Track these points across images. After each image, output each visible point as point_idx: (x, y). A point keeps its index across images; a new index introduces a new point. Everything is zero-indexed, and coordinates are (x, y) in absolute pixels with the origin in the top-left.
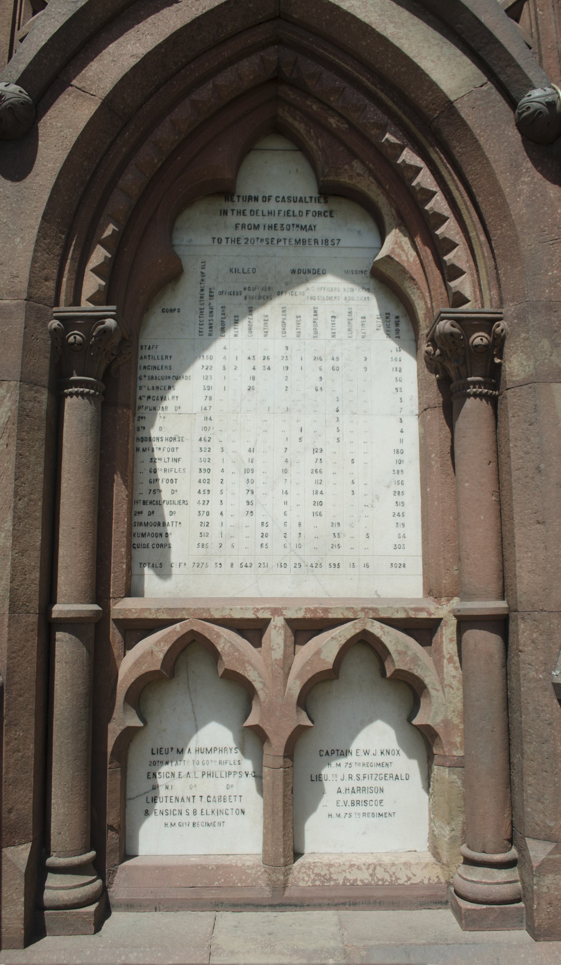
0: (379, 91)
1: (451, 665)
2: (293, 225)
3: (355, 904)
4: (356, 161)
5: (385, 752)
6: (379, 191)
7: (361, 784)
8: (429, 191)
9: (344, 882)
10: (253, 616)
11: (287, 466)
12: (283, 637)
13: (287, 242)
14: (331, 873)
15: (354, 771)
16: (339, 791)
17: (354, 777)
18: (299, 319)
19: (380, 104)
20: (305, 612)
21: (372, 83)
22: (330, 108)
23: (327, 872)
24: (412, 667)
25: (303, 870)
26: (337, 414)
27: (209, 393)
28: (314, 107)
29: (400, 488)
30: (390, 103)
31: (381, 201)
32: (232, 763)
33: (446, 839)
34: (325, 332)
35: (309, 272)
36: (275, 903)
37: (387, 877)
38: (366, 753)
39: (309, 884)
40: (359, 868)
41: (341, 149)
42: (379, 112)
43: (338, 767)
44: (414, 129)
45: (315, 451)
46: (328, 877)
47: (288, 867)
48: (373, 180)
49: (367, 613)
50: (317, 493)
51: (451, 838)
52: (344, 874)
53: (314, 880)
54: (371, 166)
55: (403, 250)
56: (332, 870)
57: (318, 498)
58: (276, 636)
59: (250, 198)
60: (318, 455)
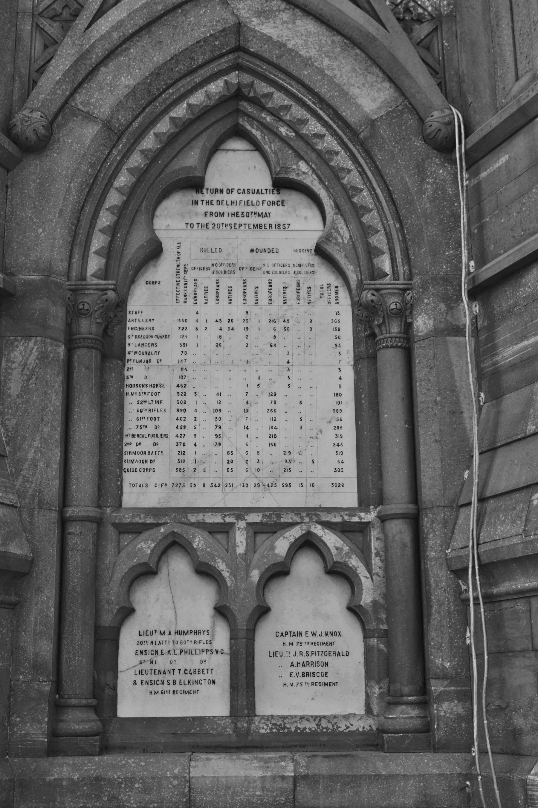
0: (318, 110)
1: (378, 558)
3: (304, 746)
6: (320, 186)
7: (310, 659)
9: (295, 730)
10: (222, 521)
11: (247, 407)
14: (285, 724)
15: (305, 648)
16: (292, 665)
17: (304, 654)
19: (319, 118)
21: (313, 103)
22: (281, 120)
23: (282, 723)
24: (347, 560)
27: (184, 349)
29: (339, 424)
30: (327, 119)
31: (323, 194)
35: (265, 251)
37: (330, 726)
38: (314, 634)
39: (268, 731)
40: (308, 720)
41: (290, 152)
42: (319, 125)
44: (346, 140)
45: (270, 394)
48: (315, 177)
49: (311, 519)
50: (272, 428)
51: (379, 694)
52: (295, 724)
54: (313, 166)
55: (340, 234)
56: (286, 721)
57: (273, 431)
58: (241, 539)
59: (216, 191)
60: (273, 398)
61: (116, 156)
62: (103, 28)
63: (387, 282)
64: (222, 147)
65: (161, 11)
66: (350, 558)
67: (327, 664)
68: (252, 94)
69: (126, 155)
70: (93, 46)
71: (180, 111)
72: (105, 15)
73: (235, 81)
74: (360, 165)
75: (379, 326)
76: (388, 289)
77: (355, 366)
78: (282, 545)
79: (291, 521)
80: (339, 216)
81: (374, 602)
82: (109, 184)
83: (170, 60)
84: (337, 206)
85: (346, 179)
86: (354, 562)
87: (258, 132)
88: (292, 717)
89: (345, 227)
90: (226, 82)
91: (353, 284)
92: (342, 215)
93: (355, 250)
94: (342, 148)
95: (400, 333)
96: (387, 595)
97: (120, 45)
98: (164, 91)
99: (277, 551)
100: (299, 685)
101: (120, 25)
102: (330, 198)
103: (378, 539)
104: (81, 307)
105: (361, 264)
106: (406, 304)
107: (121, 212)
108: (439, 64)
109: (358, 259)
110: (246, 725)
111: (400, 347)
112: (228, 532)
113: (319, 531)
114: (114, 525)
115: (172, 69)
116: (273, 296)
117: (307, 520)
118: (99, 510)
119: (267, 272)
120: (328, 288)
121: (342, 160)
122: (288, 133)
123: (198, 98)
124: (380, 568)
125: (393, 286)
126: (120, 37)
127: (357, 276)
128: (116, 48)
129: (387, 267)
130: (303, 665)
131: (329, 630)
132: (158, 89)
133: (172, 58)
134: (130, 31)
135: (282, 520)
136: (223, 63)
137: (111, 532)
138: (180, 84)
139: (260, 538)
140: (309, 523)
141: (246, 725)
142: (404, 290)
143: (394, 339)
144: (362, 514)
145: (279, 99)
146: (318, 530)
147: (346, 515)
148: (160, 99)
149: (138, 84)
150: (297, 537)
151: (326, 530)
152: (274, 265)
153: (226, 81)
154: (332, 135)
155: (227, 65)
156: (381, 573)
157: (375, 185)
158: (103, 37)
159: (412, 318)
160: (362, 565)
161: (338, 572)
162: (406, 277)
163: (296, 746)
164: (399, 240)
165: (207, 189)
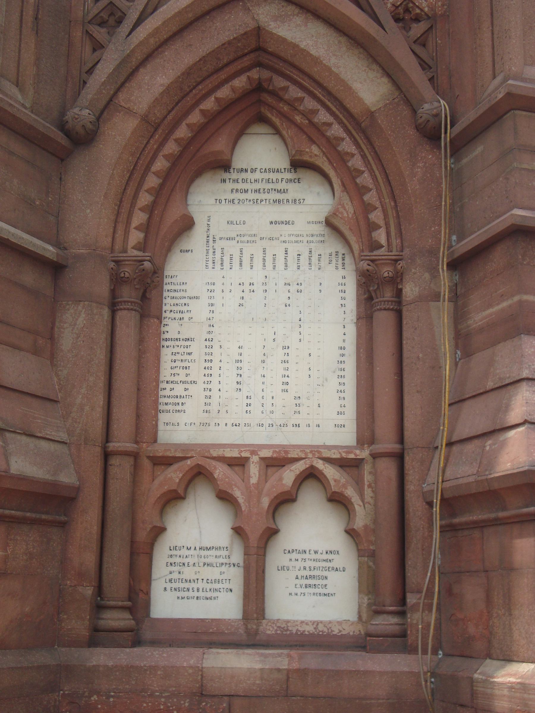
0: (327, 101)
1: (370, 489)
2: (272, 189)
3: (303, 646)
4: (314, 145)
5: (329, 552)
6: (330, 167)
7: (312, 573)
8: (360, 170)
9: (296, 633)
10: (239, 456)
11: (264, 358)
12: (258, 469)
13: (267, 201)
14: (288, 627)
15: (308, 564)
16: (297, 578)
17: (308, 569)
18: (274, 257)
19: (328, 109)
20: (273, 453)
21: (323, 95)
22: (296, 109)
23: (286, 626)
24: (343, 490)
25: (270, 624)
26: (300, 323)
27: (212, 308)
28: (285, 109)
29: (342, 373)
30: (334, 109)
31: (332, 174)
32: (224, 557)
33: (365, 605)
34: (292, 264)
35: (282, 223)
36: (250, 643)
37: (325, 630)
38: (316, 552)
39: (273, 632)
40: (307, 624)
41: (304, 137)
42: (328, 115)
43: (296, 562)
44: (350, 128)
45: (284, 348)
46: (286, 628)
47: (259, 621)
48: (326, 159)
49: (314, 455)
50: (285, 376)
51: (368, 604)
52: (297, 627)
53: (276, 630)
54: (324, 150)
55: (345, 209)
56: (289, 624)
57: (286, 380)
58: (254, 470)
59: (242, 170)
60: (286, 351)
61: (153, 145)
62: (141, 35)
63: (381, 254)
64: (246, 132)
65: (191, 18)
66: (346, 489)
67: (326, 578)
68: (271, 88)
69: (162, 144)
70: (133, 51)
71: (209, 104)
72: (143, 24)
73: (256, 76)
74: (363, 151)
75: (375, 291)
76: (382, 259)
77: (357, 323)
78: (288, 476)
79: (297, 456)
80: (345, 193)
81: (366, 527)
82: (147, 169)
83: (199, 61)
84: (343, 185)
85: (350, 162)
86: (350, 492)
87: (278, 119)
88: (294, 621)
89: (350, 203)
90: (249, 77)
91: (356, 253)
92: (347, 193)
93: (358, 224)
94: (348, 135)
95: (393, 297)
96: (375, 521)
97: (157, 49)
98: (194, 88)
99: (284, 482)
100: (303, 594)
101: (157, 30)
102: (338, 178)
103: (370, 473)
104: (122, 275)
105: (363, 235)
106: (398, 273)
107: (157, 192)
108: (433, 60)
109: (360, 231)
110: (255, 627)
111: (392, 310)
112: (244, 465)
113: (321, 465)
114: (149, 457)
115: (201, 69)
116: (288, 263)
117: (310, 456)
118: (135, 446)
119: (284, 242)
120: (336, 255)
121: (347, 146)
122: (302, 121)
123: (224, 92)
124: (372, 497)
125: (386, 257)
126: (156, 42)
127: (359, 246)
128: (153, 52)
129: (383, 240)
130: (306, 578)
131: (329, 549)
132: (189, 86)
133: (200, 60)
134: (165, 36)
135: (289, 456)
136: (246, 61)
137: (146, 464)
138: (208, 81)
139: (270, 470)
140: (312, 458)
141: (255, 627)
142: (396, 261)
143: (386, 303)
144: (358, 452)
145: (294, 92)
146: (320, 465)
147: (344, 452)
148: (191, 95)
149: (172, 83)
150: (302, 470)
151: (326, 465)
152: (290, 235)
153: (248, 76)
154: (339, 123)
155: (249, 63)
156: (372, 501)
157: (375, 168)
158: (141, 43)
159: (402, 285)
160: (356, 495)
161: (337, 500)
162: (398, 249)
163: (296, 646)
164: (393, 217)
165: (234, 169)
